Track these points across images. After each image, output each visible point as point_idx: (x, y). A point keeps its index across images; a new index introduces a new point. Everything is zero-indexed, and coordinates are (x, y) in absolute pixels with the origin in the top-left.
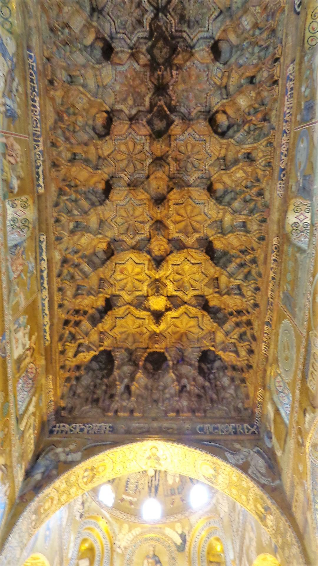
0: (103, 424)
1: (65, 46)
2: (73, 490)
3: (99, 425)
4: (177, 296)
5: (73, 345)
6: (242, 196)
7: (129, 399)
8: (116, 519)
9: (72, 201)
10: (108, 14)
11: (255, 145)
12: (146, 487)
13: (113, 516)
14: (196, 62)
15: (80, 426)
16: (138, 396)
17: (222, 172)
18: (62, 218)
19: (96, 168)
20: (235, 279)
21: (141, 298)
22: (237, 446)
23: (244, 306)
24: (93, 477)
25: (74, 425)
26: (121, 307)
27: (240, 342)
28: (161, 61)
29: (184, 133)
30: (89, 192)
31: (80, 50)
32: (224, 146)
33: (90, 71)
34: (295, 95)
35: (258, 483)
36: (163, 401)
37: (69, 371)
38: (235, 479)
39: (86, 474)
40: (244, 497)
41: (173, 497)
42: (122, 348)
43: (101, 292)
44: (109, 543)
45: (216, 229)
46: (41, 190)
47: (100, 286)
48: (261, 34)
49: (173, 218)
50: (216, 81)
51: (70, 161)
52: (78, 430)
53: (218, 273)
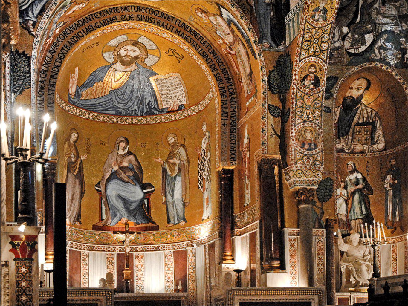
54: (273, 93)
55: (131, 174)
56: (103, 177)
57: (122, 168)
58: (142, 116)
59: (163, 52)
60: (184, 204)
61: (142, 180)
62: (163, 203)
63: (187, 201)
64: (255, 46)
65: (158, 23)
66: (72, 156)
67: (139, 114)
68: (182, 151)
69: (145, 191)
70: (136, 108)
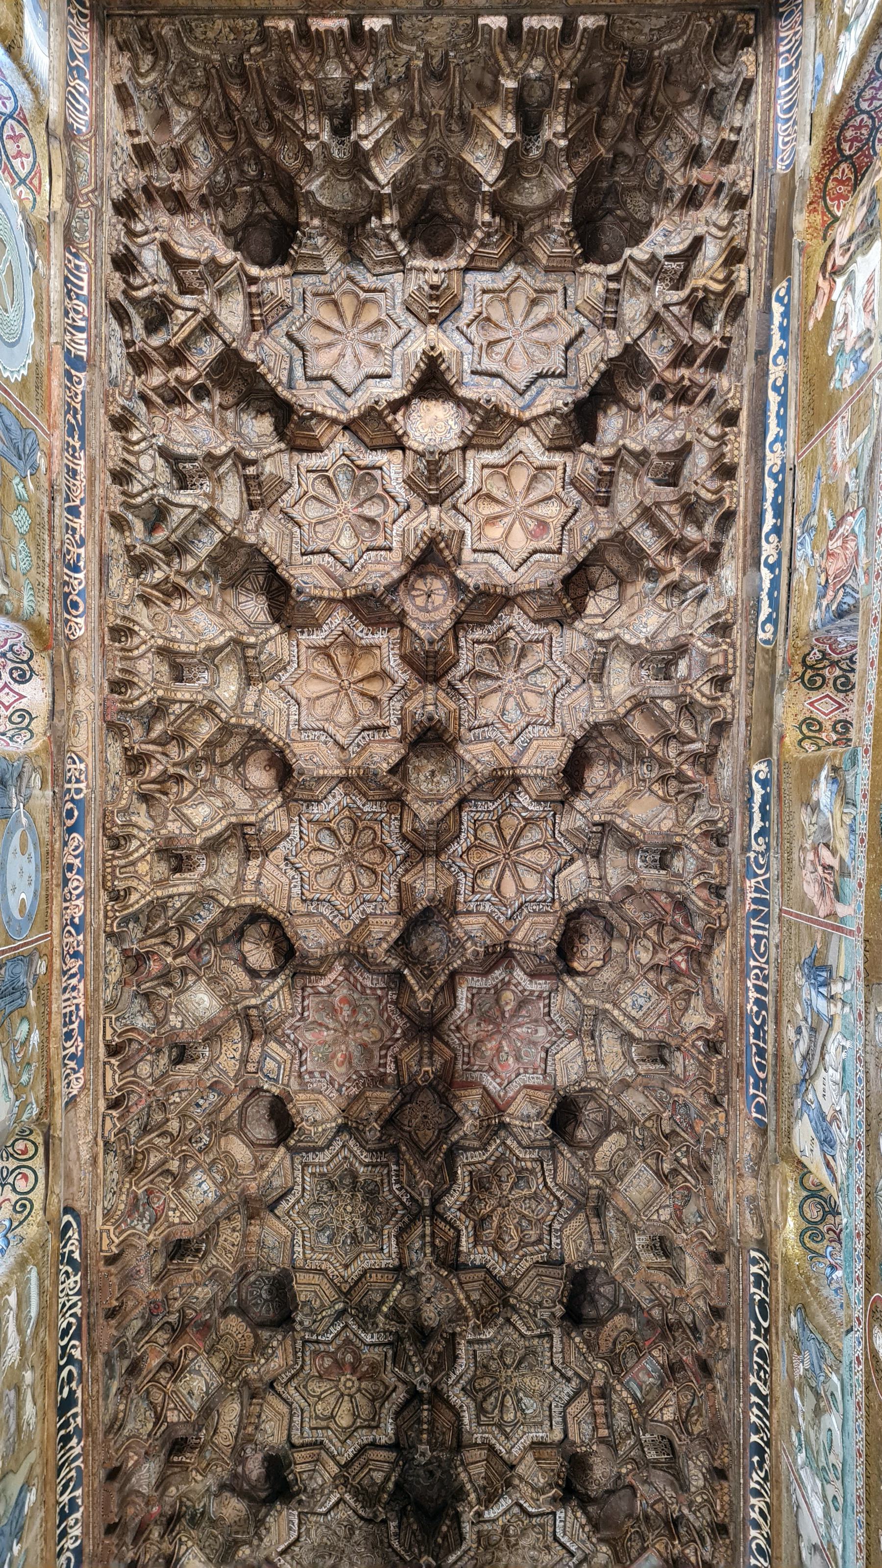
1: (673, 1132)
4: (374, 449)
5: (701, 282)
6: (189, 752)
7: (525, 83)
9: (682, 739)
10: (561, 1204)
11: (159, 893)
14: (335, 1094)
16: (492, 95)
17: (252, 819)
18: (706, 689)
19: (605, 828)
20: (194, 508)
21: (486, 442)
23: (159, 421)
26: (547, 414)
27: (163, 295)
28: (427, 1097)
29: (362, 920)
30: (630, 763)
31: (634, 1122)
32: (248, 886)
33: (610, 1074)
34: (57, 1022)
36: (408, 77)
37: (721, 185)
42: (548, 270)
43: (608, 460)
45: (263, 657)
46: (760, 768)
47: (607, 480)
48: (165, 1162)
49: (390, 688)
50: (279, 1050)
51: (678, 847)
53: (251, 526)
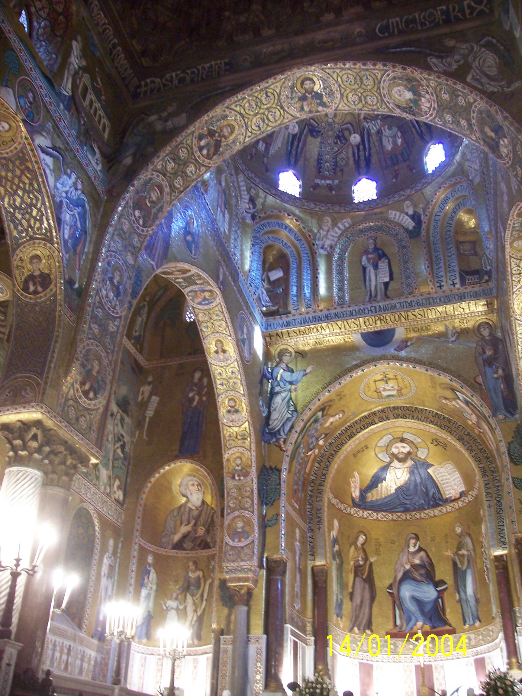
0: (213, 63)
2: (191, 168)
3: (207, 66)
8: (312, 213)
12: (351, 161)
13: (304, 211)
15: (177, 75)
22: (451, 43)
24: (218, 145)
25: (168, 76)
35: (483, 92)
38: (446, 97)
39: (203, 143)
40: (463, 123)
41: (396, 167)
44: (306, 245)
52: (176, 82)
54: (517, 464)
55: (423, 571)
56: (395, 578)
57: (414, 566)
58: (429, 508)
59: (429, 443)
60: (477, 601)
61: (435, 577)
62: (457, 602)
63: (479, 596)
64: (490, 420)
65: (413, 418)
66: (360, 559)
67: (426, 507)
68: (468, 540)
69: (438, 589)
70: (422, 501)
